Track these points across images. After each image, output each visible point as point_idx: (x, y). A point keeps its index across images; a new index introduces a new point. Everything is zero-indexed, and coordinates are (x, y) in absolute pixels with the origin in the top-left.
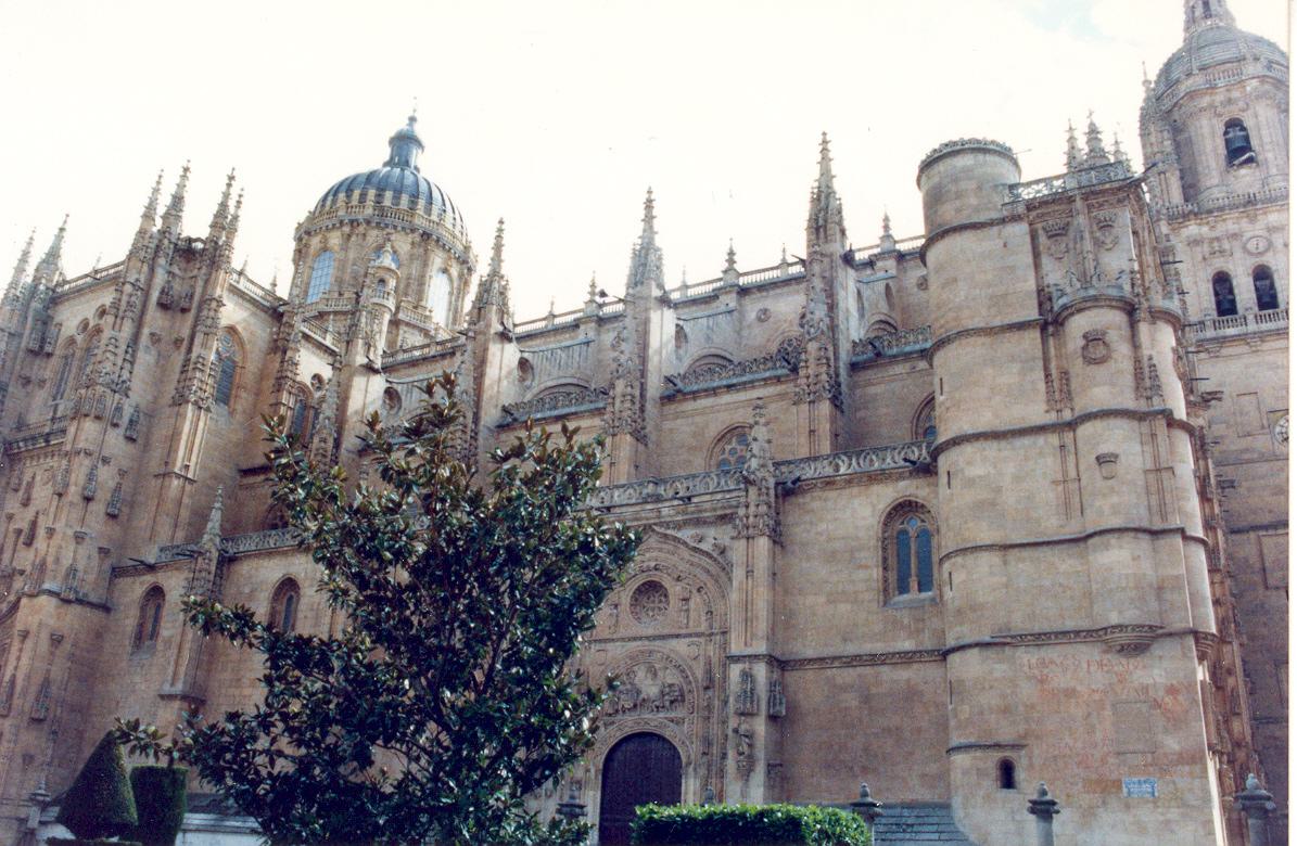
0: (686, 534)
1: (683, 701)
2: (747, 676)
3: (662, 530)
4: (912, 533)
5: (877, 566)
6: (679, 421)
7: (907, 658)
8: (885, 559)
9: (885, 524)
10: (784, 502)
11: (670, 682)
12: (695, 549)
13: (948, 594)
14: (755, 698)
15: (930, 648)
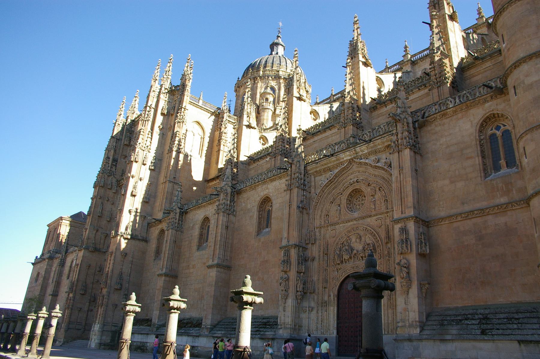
0: (371, 160)
1: (376, 252)
2: (404, 230)
3: (358, 161)
4: (499, 133)
5: (478, 156)
6: (379, 119)
7: (503, 208)
8: (482, 152)
9: (480, 131)
10: (420, 131)
11: (368, 242)
12: (376, 167)
13: (525, 161)
14: (409, 243)
15: (518, 199)
